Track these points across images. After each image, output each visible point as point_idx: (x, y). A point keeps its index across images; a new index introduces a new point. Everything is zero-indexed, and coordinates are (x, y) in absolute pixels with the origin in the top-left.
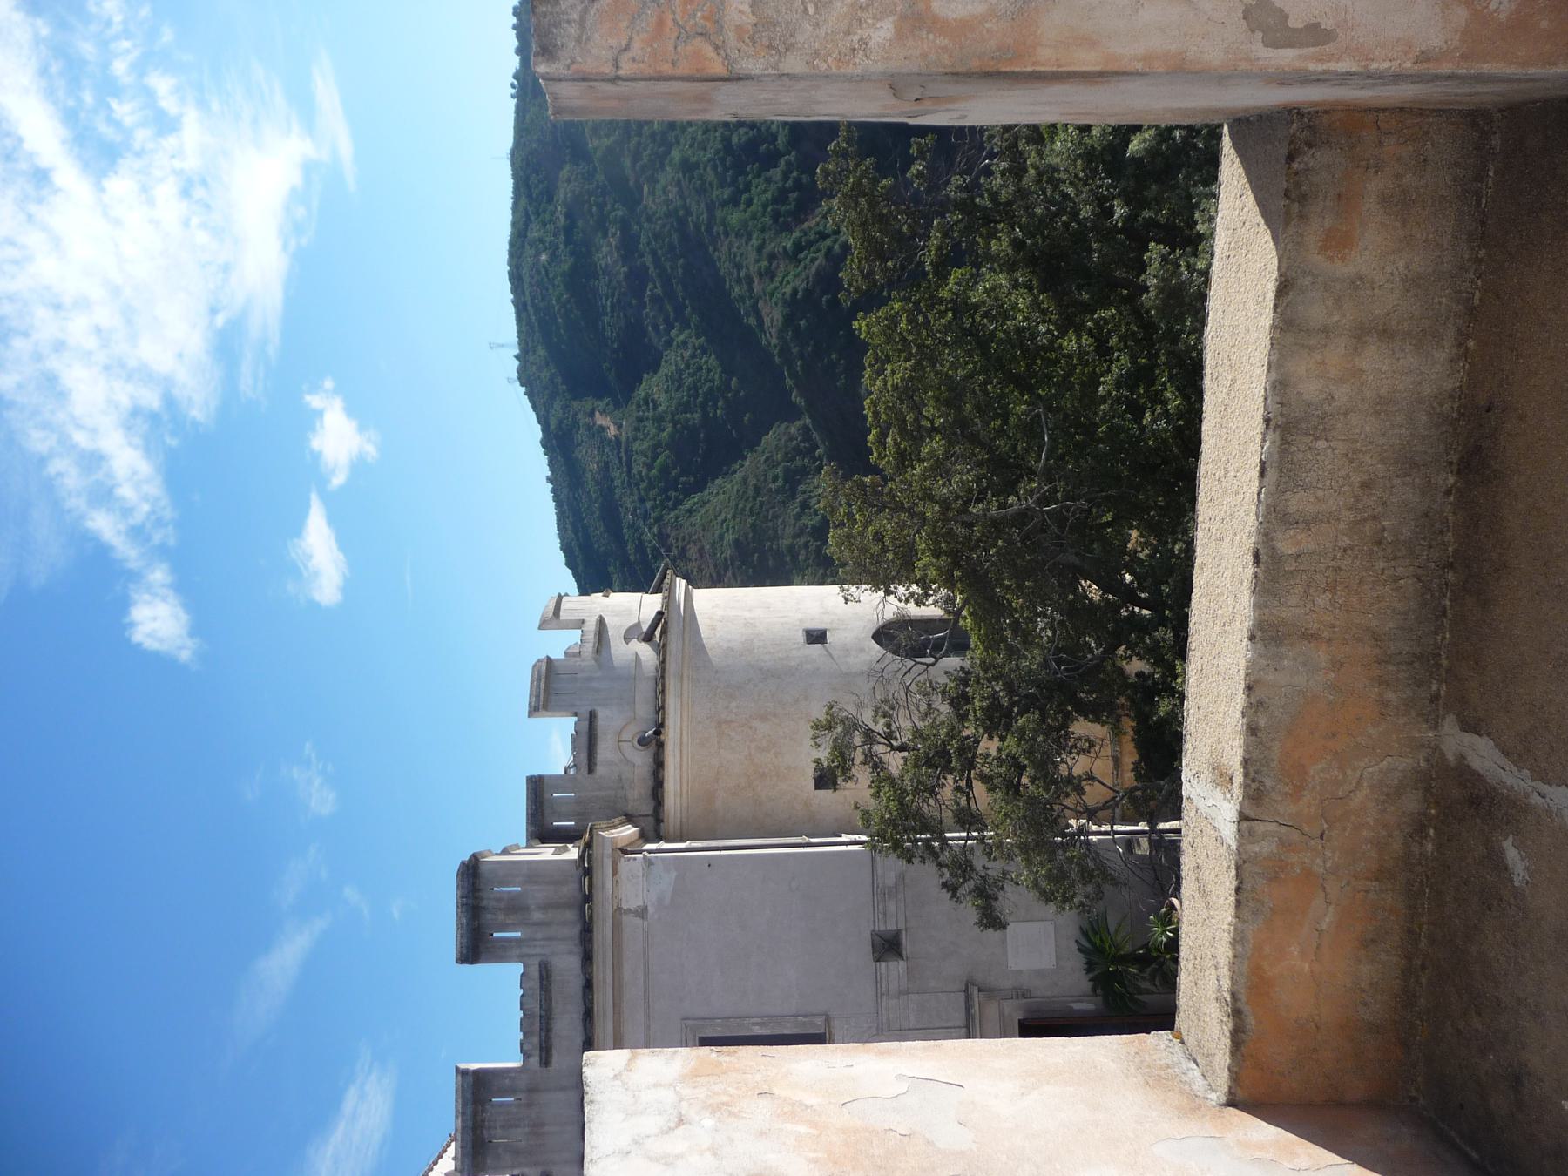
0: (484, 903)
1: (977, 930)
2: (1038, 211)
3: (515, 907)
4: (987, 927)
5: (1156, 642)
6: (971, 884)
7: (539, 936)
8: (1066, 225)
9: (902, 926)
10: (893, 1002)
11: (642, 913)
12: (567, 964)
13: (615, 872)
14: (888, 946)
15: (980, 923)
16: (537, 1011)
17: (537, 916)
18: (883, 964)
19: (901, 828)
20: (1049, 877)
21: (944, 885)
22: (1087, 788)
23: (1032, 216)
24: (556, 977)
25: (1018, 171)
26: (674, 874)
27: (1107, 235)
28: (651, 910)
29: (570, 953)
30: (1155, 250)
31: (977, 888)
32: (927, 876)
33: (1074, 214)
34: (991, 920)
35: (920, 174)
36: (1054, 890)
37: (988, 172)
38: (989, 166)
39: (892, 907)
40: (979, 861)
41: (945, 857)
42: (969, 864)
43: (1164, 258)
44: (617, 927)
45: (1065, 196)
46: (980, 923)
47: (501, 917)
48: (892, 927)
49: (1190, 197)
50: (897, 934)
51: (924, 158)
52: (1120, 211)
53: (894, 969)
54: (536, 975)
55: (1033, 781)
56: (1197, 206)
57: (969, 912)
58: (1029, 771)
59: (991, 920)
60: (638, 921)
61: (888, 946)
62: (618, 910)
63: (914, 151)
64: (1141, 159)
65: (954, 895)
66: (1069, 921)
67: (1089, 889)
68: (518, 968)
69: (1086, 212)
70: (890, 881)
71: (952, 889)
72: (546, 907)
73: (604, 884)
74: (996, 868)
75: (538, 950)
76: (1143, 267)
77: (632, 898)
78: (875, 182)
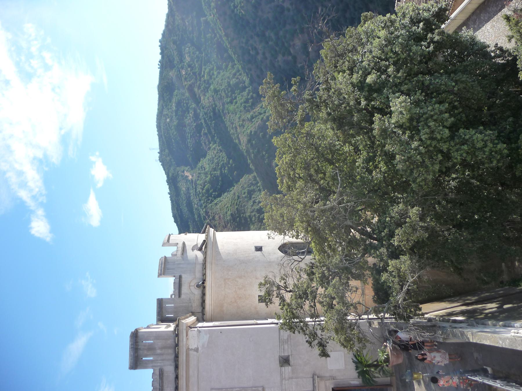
0: (139, 347)
1: (319, 357)
2: (336, 103)
3: (151, 349)
4: (323, 356)
5: (381, 253)
6: (316, 342)
7: (160, 359)
8: (345, 107)
9: (290, 354)
10: (287, 382)
11: (197, 350)
12: (169, 369)
13: (187, 335)
14: (285, 361)
15: (320, 355)
16: (158, 387)
17: (159, 351)
18: (283, 368)
19: (292, 323)
20: (345, 339)
21: (307, 341)
22: (358, 307)
23: (334, 104)
24: (165, 374)
25: (328, 89)
26: (208, 335)
27: (360, 111)
28: (200, 349)
29: (171, 365)
30: (377, 116)
31: (319, 343)
32: (301, 338)
33: (348, 104)
34: (324, 354)
35: (295, 90)
36: (347, 343)
37: (318, 90)
38: (318, 87)
39: (286, 347)
40: (319, 332)
41: (307, 332)
42: (315, 333)
43: (380, 119)
44: (188, 355)
45: (344, 98)
46: (320, 355)
47: (145, 352)
48: (286, 354)
49: (388, 98)
50: (288, 356)
51: (296, 85)
52: (363, 103)
53: (287, 370)
54: (157, 373)
55: (338, 303)
56: (391, 101)
57: (317, 351)
58: (337, 300)
59: (324, 354)
60: (195, 353)
61: (285, 361)
62: (188, 349)
63: (293, 82)
64: (371, 84)
65: (311, 345)
66: (351, 355)
67: (360, 345)
68: (151, 371)
69: (352, 103)
70: (286, 337)
71: (310, 343)
72: (163, 348)
73: (183, 340)
74: (326, 335)
75: (159, 364)
76: (372, 122)
77: (193, 345)
78: (279, 92)
